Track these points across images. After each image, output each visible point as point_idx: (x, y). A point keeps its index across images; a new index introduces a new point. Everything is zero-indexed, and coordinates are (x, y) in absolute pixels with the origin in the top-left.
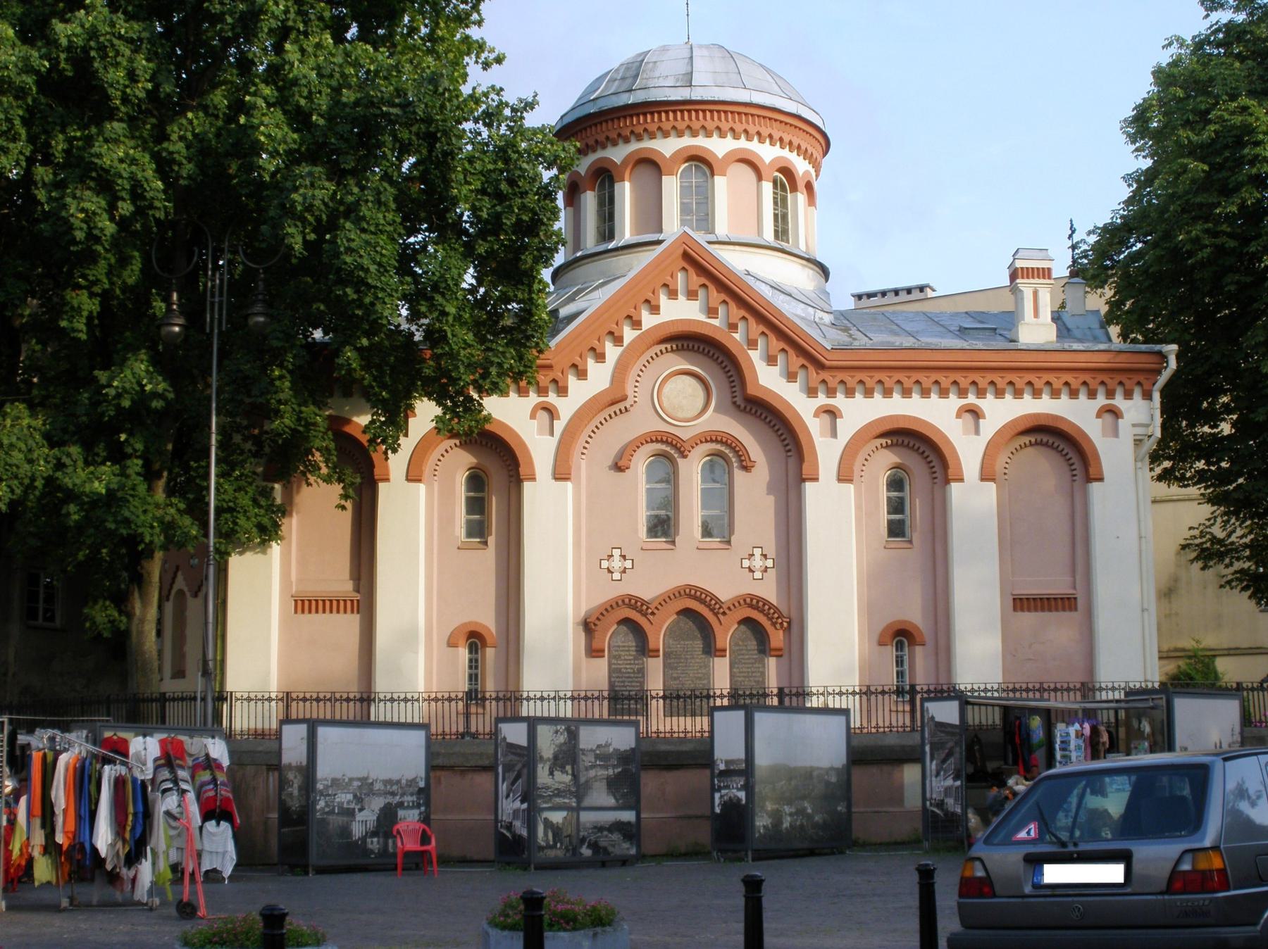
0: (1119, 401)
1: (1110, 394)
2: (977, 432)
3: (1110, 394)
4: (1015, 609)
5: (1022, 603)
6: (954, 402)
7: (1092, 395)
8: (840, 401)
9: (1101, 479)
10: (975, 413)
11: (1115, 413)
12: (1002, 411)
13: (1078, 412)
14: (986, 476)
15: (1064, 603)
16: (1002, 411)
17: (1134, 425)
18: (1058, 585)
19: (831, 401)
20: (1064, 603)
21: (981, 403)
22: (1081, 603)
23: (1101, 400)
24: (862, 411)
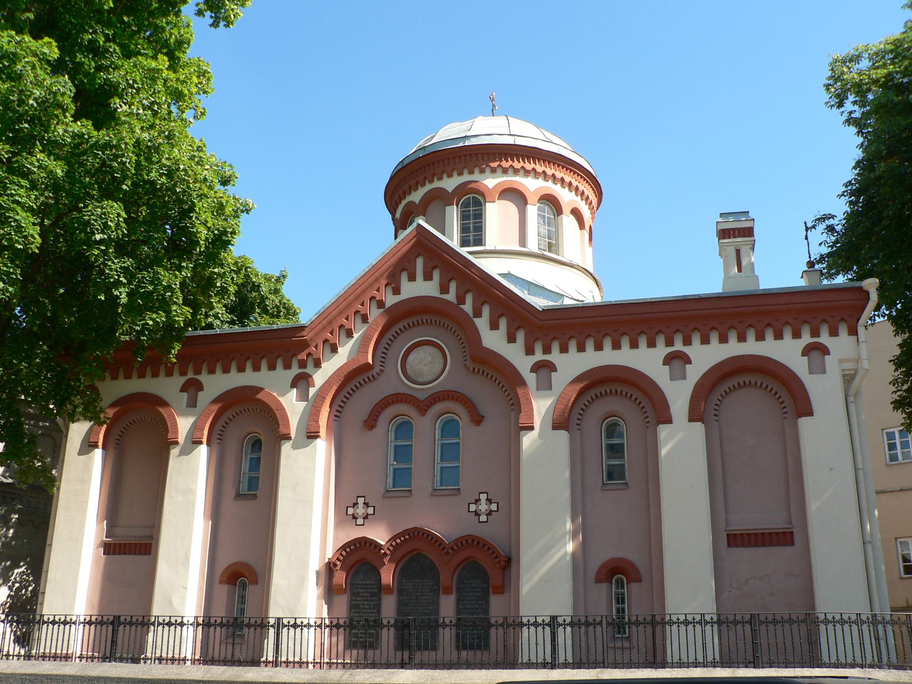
0: (824, 338)
1: (815, 333)
2: (684, 377)
3: (815, 333)
4: (729, 545)
5: (737, 539)
6: (662, 350)
7: (797, 335)
8: (555, 356)
9: (811, 414)
10: (686, 359)
11: (825, 351)
12: (706, 355)
13: (786, 350)
14: (693, 417)
15: (783, 538)
16: (706, 355)
17: (841, 361)
18: (770, 519)
19: (547, 357)
20: (783, 538)
21: (687, 350)
22: (797, 537)
23: (806, 339)
24: (573, 364)
